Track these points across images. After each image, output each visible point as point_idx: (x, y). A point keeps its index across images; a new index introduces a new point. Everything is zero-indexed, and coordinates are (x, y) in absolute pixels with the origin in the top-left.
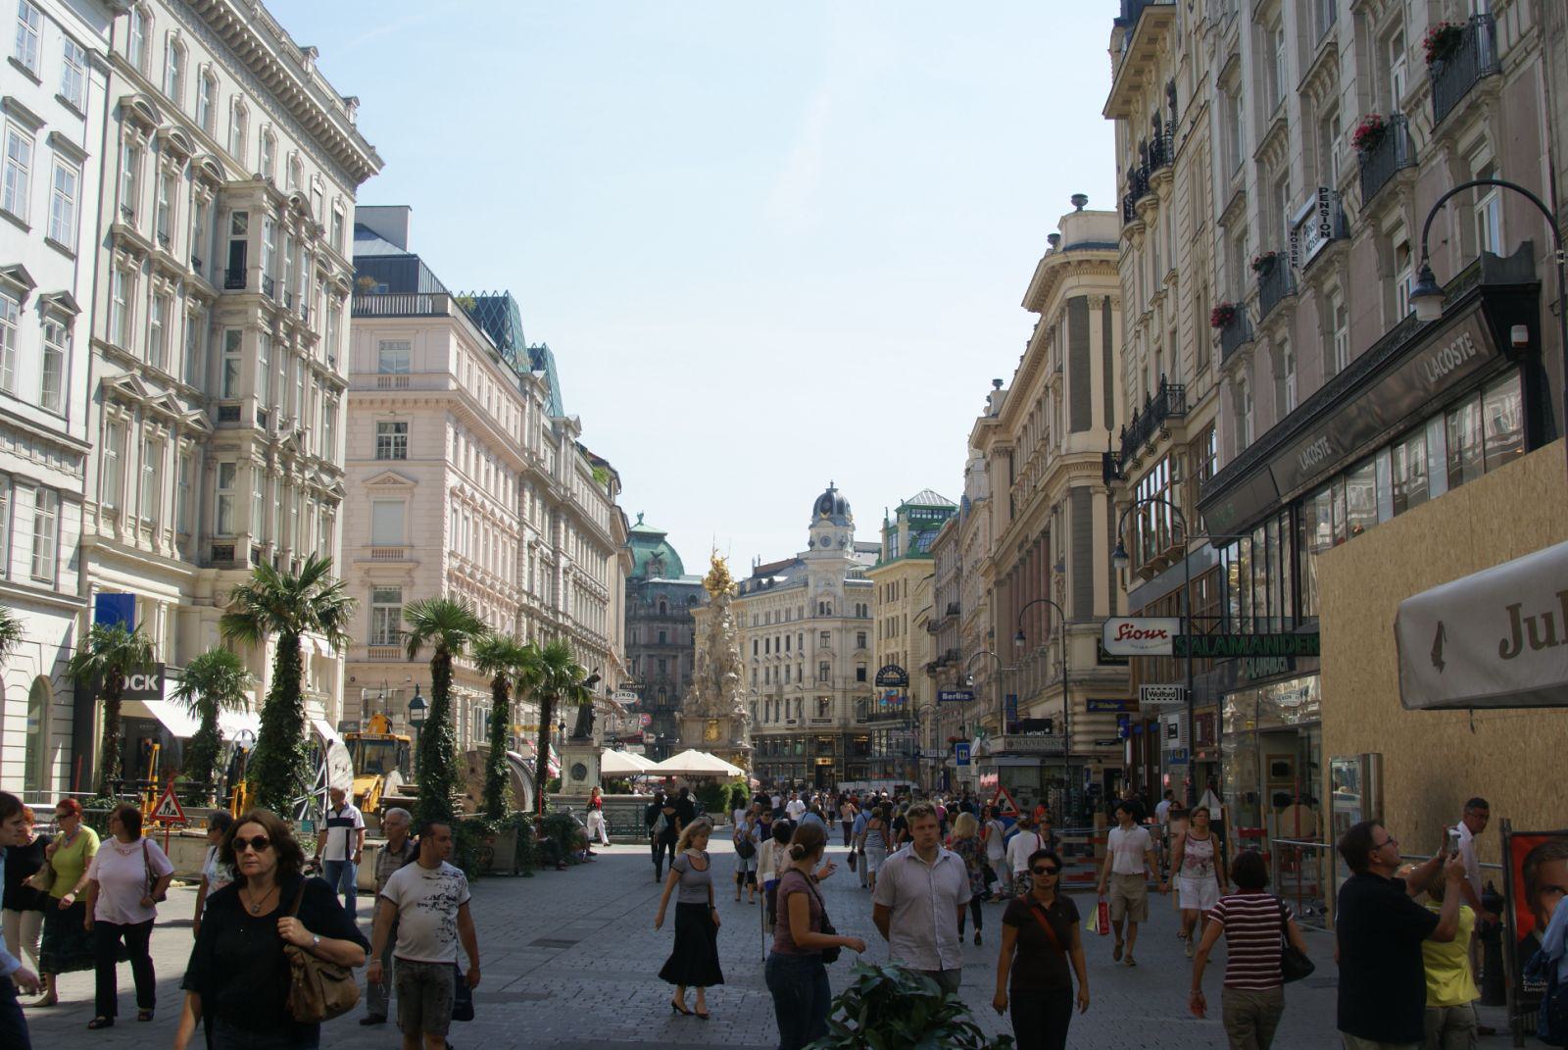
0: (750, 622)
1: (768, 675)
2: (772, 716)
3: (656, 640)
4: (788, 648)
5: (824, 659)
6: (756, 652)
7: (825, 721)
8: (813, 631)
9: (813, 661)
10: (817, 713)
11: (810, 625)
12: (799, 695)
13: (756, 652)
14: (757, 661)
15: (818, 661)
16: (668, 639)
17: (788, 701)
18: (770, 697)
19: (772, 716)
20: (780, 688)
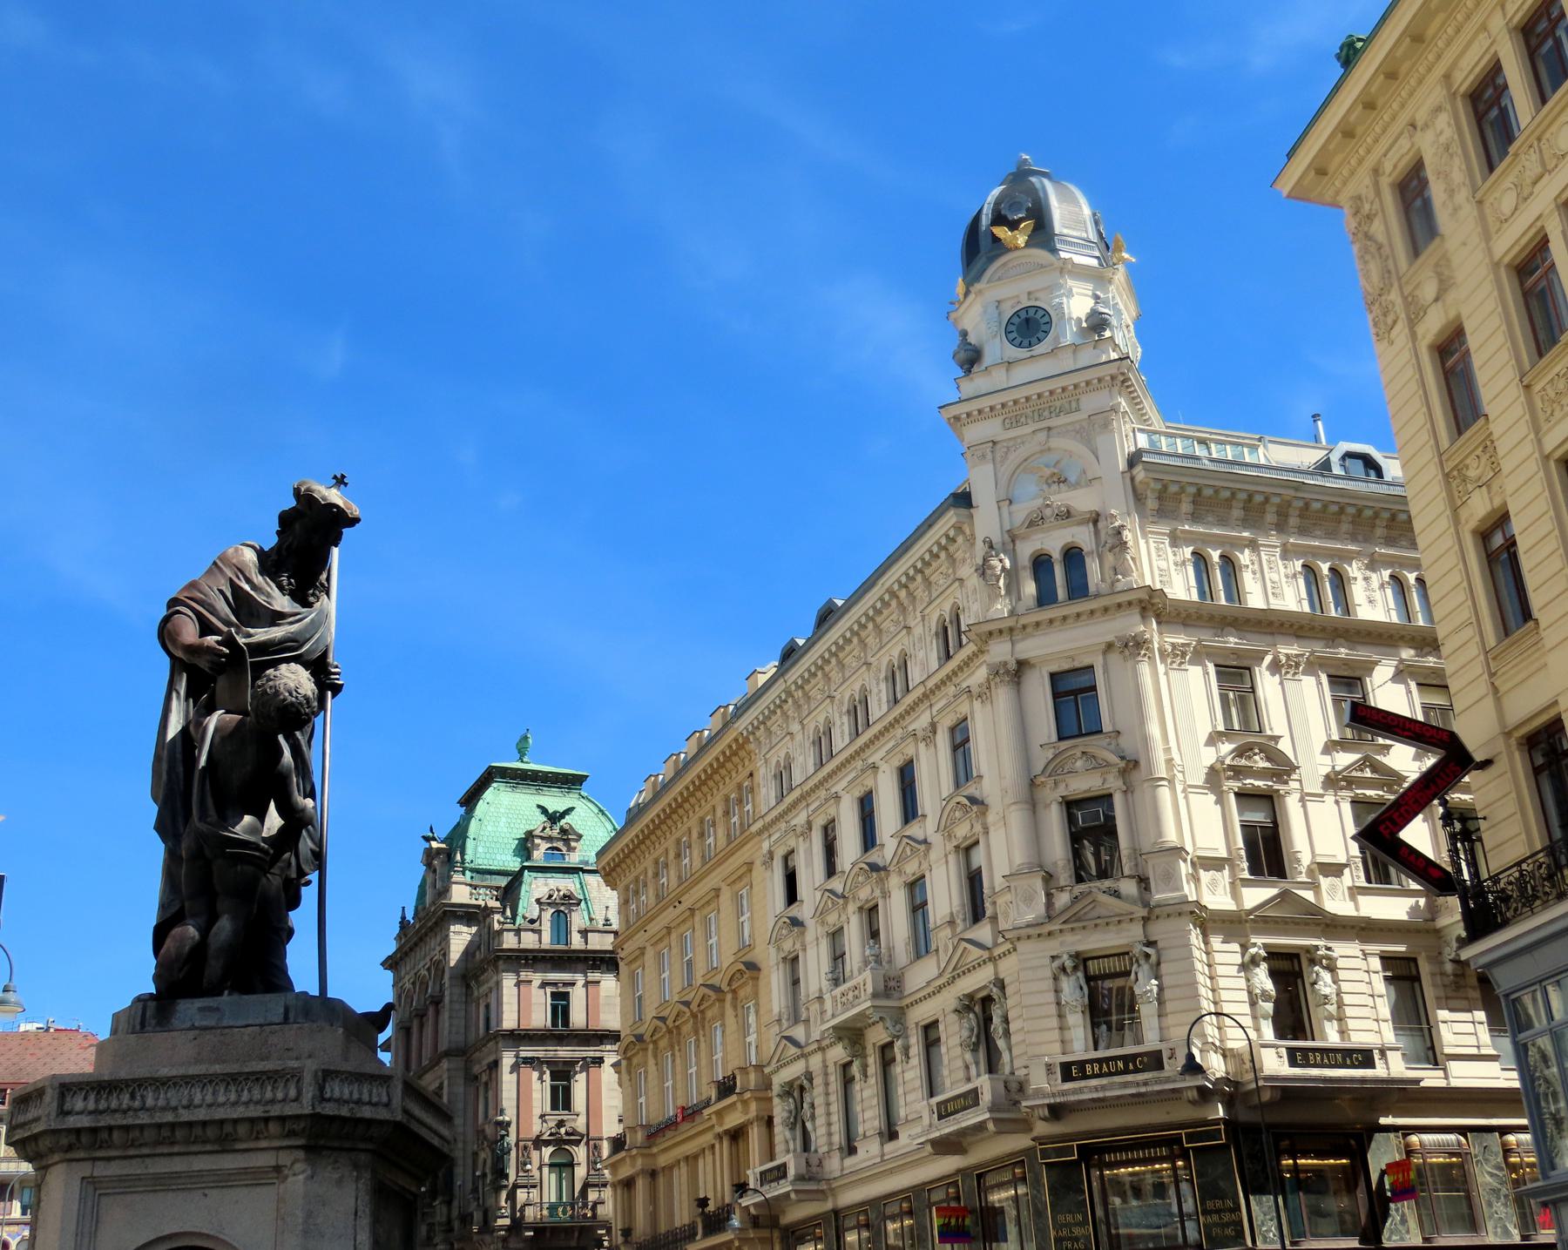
0: (767, 793)
1: (838, 957)
2: (869, 1117)
3: (540, 1017)
4: (910, 811)
5: (1083, 784)
6: (792, 896)
7: (1131, 1064)
8: (1018, 671)
9: (1033, 804)
10: (1080, 1045)
11: (1000, 651)
12: (977, 980)
13: (792, 896)
14: (796, 922)
15: (1051, 797)
16: (578, 1018)
17: (930, 1029)
18: (852, 1034)
19: (869, 1117)
20: (890, 986)
